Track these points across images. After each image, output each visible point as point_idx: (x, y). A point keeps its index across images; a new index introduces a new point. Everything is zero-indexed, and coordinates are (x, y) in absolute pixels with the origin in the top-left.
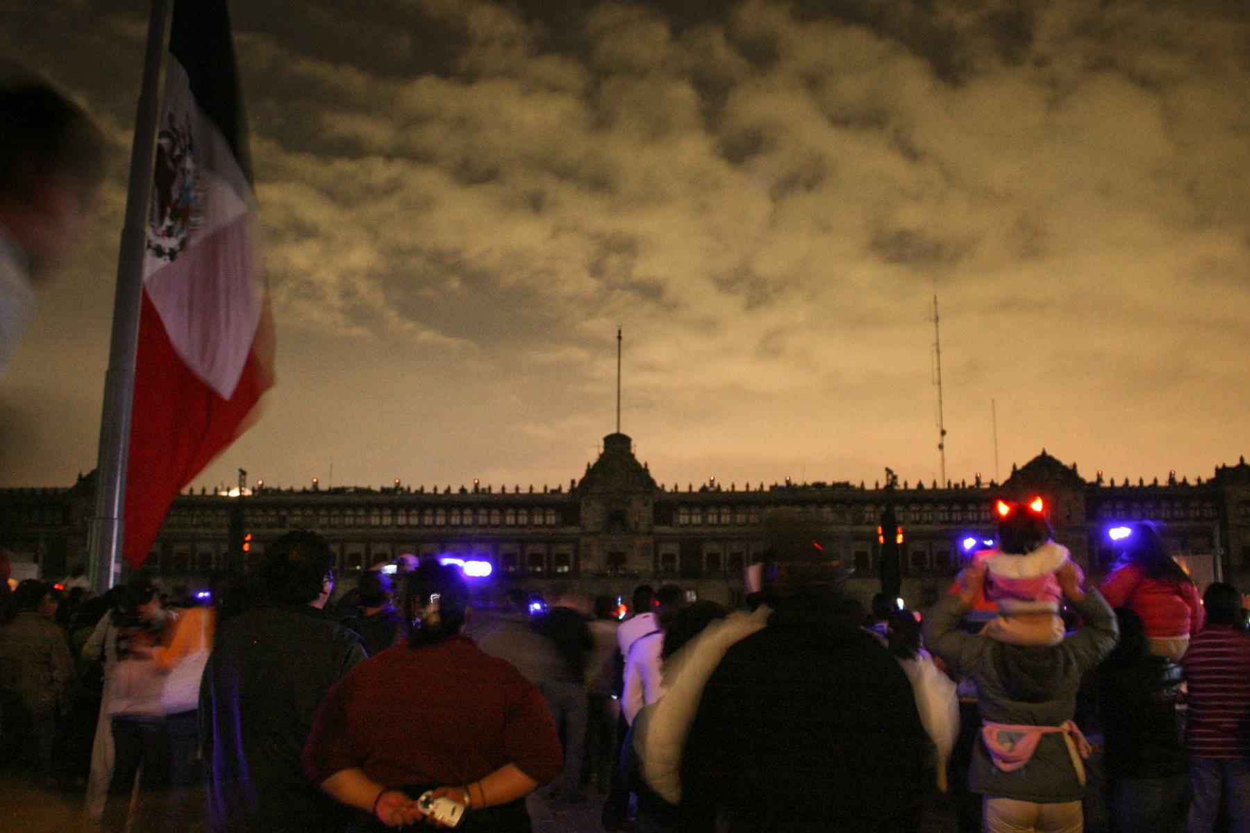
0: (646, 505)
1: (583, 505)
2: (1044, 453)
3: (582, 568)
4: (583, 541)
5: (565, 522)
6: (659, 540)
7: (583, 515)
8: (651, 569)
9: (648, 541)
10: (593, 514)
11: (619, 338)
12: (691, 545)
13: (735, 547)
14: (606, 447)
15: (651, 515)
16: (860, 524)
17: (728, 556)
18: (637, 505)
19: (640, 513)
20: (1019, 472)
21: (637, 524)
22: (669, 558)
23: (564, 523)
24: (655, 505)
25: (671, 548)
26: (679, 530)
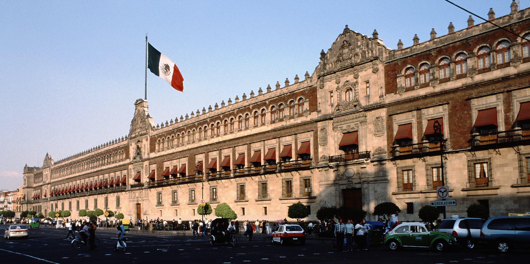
2: (347, 30)
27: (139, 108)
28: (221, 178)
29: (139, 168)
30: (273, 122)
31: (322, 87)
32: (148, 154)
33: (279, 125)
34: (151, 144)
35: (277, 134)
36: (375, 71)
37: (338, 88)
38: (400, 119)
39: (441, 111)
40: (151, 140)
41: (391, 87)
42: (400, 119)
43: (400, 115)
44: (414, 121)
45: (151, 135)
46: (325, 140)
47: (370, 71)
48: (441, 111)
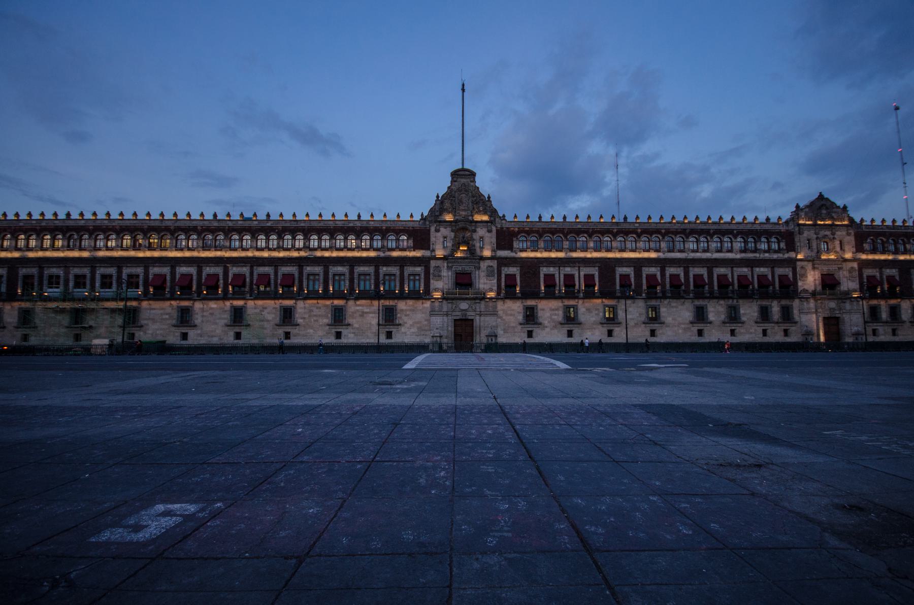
0: (490, 231)
1: (433, 229)
2: (821, 197)
4: (433, 263)
6: (503, 262)
7: (433, 239)
9: (494, 264)
11: (463, 90)
12: (531, 268)
13: (568, 270)
15: (494, 240)
16: (673, 251)
17: (562, 276)
18: (481, 232)
20: (802, 209)
21: (482, 248)
22: (510, 278)
23: (415, 248)
25: (514, 270)
28: (664, 297)
30: (741, 251)
31: (800, 233)
32: (493, 251)
33: (750, 255)
34: (497, 238)
35: (751, 264)
36: (849, 234)
37: (817, 238)
38: (868, 272)
39: (894, 272)
41: (859, 249)
42: (868, 272)
44: (878, 274)
45: (499, 226)
46: (804, 276)
47: (844, 233)
48: (894, 272)
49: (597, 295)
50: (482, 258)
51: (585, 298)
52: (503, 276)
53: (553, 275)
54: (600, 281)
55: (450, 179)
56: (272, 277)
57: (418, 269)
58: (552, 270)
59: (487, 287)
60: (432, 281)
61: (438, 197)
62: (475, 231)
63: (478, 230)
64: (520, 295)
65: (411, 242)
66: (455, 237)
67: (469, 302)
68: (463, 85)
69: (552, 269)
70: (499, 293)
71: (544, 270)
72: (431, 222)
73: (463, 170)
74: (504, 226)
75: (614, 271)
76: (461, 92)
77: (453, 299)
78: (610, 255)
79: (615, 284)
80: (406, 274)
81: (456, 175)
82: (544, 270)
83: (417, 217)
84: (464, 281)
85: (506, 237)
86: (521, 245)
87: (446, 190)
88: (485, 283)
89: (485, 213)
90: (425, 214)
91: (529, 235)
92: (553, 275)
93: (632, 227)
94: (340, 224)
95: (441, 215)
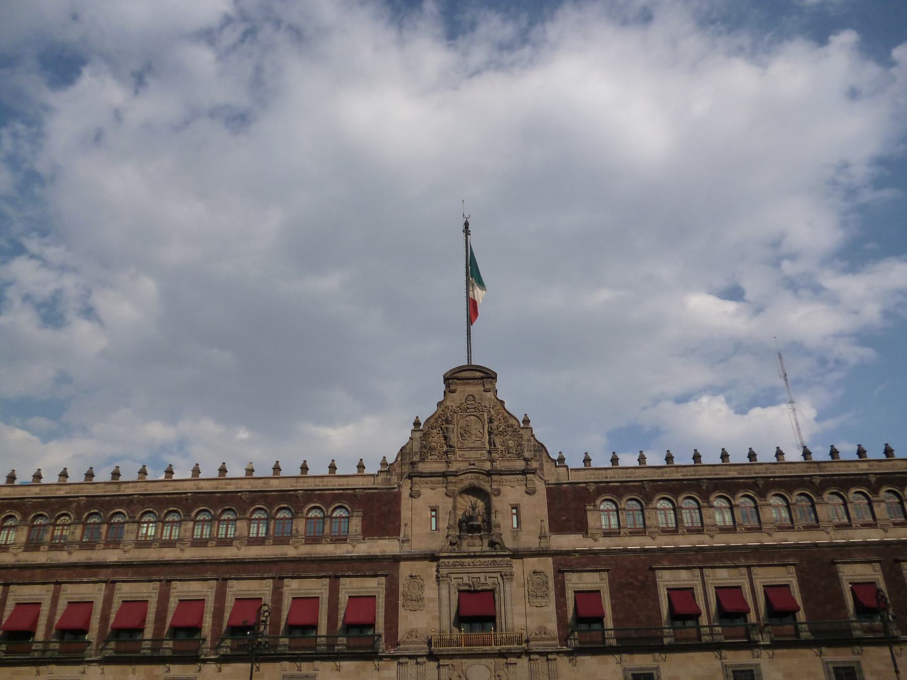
0: (530, 492)
1: (405, 492)
3: (403, 627)
4: (405, 568)
5: (371, 530)
6: (566, 563)
7: (405, 514)
8: (552, 626)
9: (547, 565)
10: (425, 518)
11: (467, 231)
12: (633, 573)
13: (723, 576)
14: (449, 391)
15: (544, 512)
19: (520, 510)
22: (588, 596)
24: (549, 491)
26: (603, 544)
27: (463, 391)
29: (481, 576)
34: (550, 505)
40: (556, 494)
43: (134, 584)
49: (805, 635)
50: (517, 555)
51: (775, 645)
52: (570, 596)
53: (690, 590)
54: (805, 601)
55: (443, 387)
56: (45, 610)
57: (373, 586)
58: (683, 578)
59: (533, 624)
60: (402, 612)
61: (417, 424)
62: (498, 493)
63: (505, 489)
64: (614, 642)
65: (356, 524)
66: (455, 508)
67: (490, 662)
68: (466, 225)
69: (684, 575)
70: (564, 640)
71: (667, 579)
72: (401, 476)
73: (470, 368)
74: (564, 480)
75: (835, 577)
76: (463, 235)
77: (451, 656)
78: (822, 538)
79: (843, 606)
80: (343, 598)
81: (452, 379)
82: (667, 579)
83: (372, 468)
84: (476, 613)
85: (570, 504)
86: (604, 521)
87: (434, 408)
88: (527, 612)
89: (520, 455)
90: (391, 460)
91: (620, 497)
92: (690, 590)
93: (852, 470)
94: (207, 487)
95: (423, 460)
